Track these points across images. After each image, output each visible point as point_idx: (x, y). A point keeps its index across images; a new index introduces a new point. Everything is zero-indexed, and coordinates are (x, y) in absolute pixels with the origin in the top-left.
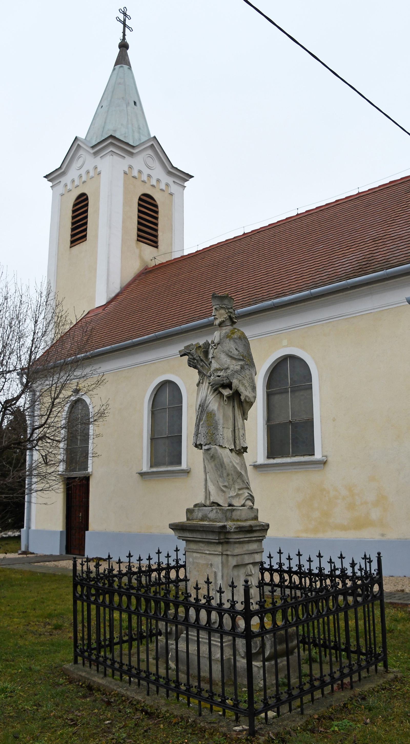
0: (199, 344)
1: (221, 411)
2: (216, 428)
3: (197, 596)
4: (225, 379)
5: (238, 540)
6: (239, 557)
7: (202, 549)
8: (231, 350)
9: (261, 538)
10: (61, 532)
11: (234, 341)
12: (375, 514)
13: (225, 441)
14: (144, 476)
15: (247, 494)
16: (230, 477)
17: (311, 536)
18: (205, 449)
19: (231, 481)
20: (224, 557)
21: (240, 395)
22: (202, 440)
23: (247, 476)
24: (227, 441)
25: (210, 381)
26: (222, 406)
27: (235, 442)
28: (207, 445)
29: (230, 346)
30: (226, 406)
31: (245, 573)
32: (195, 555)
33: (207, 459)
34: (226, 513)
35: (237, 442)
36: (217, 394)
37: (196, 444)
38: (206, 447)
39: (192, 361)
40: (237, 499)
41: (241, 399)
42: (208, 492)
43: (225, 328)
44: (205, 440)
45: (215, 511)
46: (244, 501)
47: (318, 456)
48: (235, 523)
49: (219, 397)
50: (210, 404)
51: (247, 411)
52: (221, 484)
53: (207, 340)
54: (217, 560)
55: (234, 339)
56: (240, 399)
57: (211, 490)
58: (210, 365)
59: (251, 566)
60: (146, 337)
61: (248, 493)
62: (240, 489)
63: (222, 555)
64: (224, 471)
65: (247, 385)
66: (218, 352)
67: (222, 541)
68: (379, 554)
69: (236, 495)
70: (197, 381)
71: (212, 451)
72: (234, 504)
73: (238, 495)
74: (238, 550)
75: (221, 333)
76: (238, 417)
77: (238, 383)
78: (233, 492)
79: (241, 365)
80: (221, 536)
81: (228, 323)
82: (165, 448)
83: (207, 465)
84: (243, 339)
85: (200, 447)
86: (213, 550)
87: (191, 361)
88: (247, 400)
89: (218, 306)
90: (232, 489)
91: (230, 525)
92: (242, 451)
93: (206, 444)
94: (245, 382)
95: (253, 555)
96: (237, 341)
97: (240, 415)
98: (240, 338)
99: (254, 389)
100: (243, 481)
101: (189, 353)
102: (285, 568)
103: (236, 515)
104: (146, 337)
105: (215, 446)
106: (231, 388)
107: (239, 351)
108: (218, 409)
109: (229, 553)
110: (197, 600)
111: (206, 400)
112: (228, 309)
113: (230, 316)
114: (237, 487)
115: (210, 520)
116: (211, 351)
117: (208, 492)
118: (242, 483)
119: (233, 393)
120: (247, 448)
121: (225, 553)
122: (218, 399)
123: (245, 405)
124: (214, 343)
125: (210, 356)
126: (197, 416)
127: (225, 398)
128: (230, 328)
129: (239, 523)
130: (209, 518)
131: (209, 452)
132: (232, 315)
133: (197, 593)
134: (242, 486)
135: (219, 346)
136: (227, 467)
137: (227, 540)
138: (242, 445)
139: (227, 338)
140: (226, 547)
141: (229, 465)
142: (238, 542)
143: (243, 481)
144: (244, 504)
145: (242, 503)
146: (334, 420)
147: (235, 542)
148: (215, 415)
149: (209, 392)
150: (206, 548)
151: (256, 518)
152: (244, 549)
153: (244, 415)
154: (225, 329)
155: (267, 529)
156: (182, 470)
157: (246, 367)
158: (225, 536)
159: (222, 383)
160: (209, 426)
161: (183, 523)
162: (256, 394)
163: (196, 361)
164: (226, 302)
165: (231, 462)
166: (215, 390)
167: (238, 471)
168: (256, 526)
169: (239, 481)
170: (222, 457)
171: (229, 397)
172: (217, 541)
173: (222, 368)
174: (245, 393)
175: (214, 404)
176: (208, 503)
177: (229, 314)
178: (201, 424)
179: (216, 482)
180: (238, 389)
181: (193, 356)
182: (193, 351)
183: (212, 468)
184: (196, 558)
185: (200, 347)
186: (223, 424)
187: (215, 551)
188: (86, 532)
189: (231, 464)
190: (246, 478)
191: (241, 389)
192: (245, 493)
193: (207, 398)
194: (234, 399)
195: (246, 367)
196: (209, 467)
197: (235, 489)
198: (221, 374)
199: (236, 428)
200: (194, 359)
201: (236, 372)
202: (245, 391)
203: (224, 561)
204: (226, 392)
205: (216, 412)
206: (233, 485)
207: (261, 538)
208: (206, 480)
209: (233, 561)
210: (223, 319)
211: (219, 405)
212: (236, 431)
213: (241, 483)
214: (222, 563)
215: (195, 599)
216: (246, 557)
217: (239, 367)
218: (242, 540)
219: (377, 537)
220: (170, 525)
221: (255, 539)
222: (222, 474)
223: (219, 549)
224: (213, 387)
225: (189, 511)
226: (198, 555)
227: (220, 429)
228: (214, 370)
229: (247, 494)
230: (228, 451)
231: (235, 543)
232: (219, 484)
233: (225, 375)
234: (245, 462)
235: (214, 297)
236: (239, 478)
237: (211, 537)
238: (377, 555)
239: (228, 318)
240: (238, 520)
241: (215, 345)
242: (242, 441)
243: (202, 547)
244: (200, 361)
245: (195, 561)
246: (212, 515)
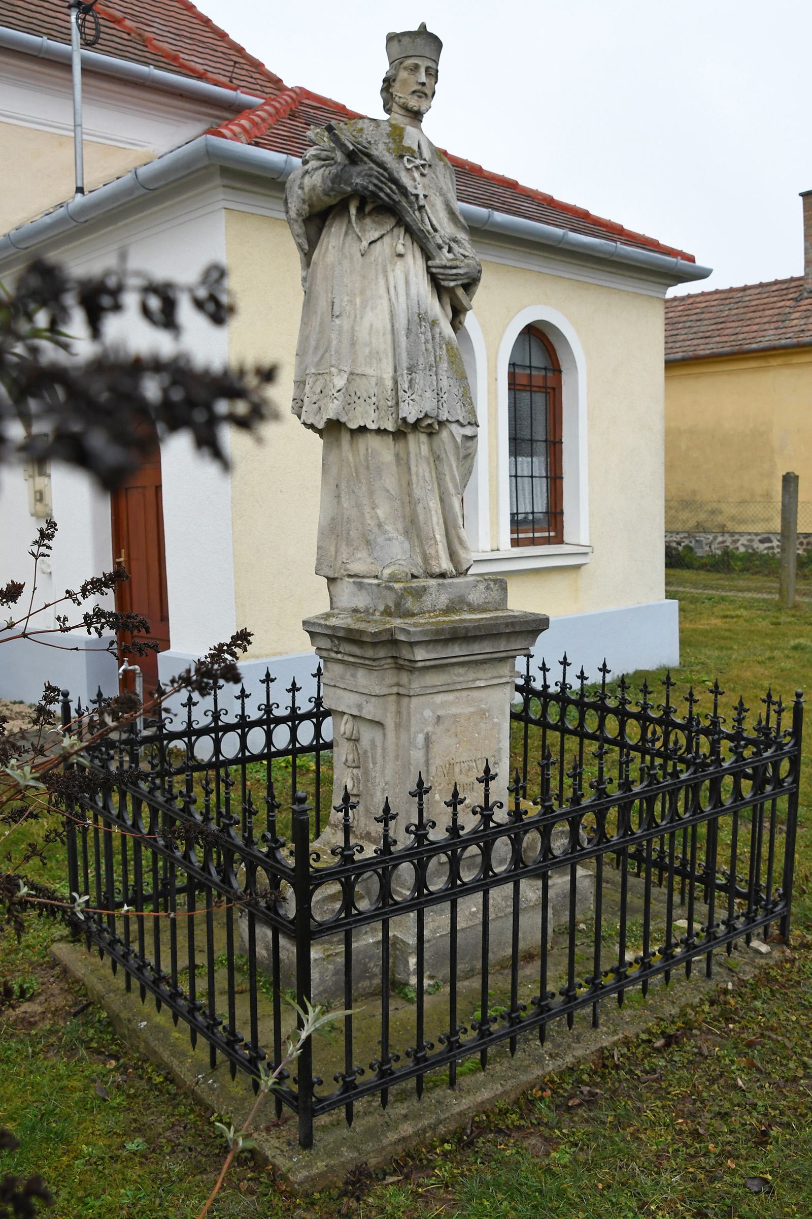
7: (461, 679)
28: (469, 427)
32: (439, 698)
115: (472, 609)
130: (469, 605)
150: (471, 675)
184: (443, 705)
187: (501, 677)
226: (450, 697)
243: (459, 675)
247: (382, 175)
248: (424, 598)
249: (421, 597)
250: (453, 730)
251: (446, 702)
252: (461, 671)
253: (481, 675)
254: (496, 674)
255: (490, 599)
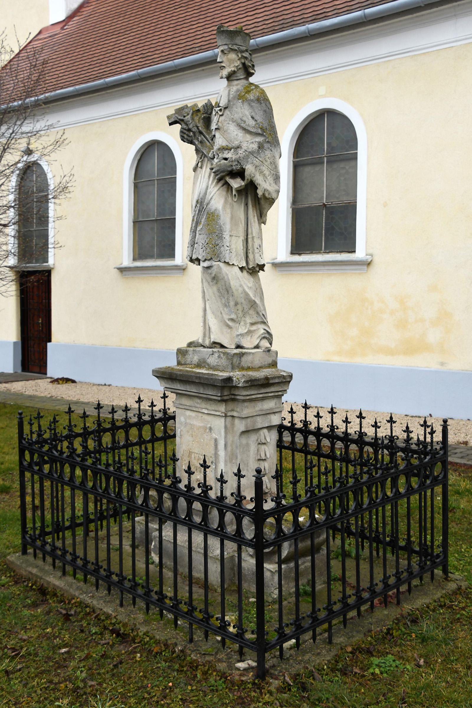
0: (197, 106)
1: (229, 211)
2: (220, 237)
3: (189, 482)
4: (234, 164)
5: (248, 398)
6: (249, 420)
7: (198, 406)
8: (244, 119)
9: (280, 393)
10: (15, 343)
11: (249, 104)
12: (434, 336)
13: (233, 256)
14: (124, 273)
15: (263, 331)
16: (239, 307)
17: (346, 360)
18: (204, 267)
19: (240, 311)
20: (229, 419)
21: (257, 188)
22: (200, 254)
23: (263, 305)
24: (236, 255)
25: (213, 167)
26: (230, 204)
27: (247, 257)
29: (243, 111)
30: (235, 204)
31: (257, 440)
32: (188, 413)
33: (207, 280)
34: (232, 359)
35: (251, 256)
36: (223, 186)
37: (191, 258)
38: (206, 264)
39: (187, 133)
40: (249, 338)
41: (257, 194)
42: (207, 327)
43: (236, 82)
44: (204, 254)
45: (216, 355)
46: (258, 341)
47: (360, 253)
48: (244, 373)
49: (226, 189)
50: (213, 200)
51: (266, 211)
52: (226, 317)
53: (209, 100)
54: (219, 424)
55: (249, 102)
56: (256, 194)
57: (211, 326)
58: (212, 140)
59: (265, 431)
60: (124, 76)
61: (265, 329)
62: (252, 324)
63: (226, 416)
64: (231, 298)
65: (267, 173)
66: (225, 121)
67: (225, 398)
68: (445, 421)
69: (246, 333)
70: (194, 163)
71: (214, 271)
72: (244, 345)
73: (249, 332)
74: (247, 410)
75: (229, 91)
76: (252, 221)
77: (254, 171)
78: (244, 328)
79: (259, 143)
80: (225, 392)
81: (241, 75)
82: (153, 235)
83: (207, 290)
84: (263, 101)
85: (196, 262)
86: (213, 409)
87: (185, 133)
88: (267, 195)
89: (226, 47)
90: (242, 323)
91: (238, 376)
92: (258, 269)
93: (205, 260)
94: (264, 168)
95: (268, 416)
96: (253, 104)
97: (256, 218)
98: (258, 100)
99: (277, 178)
100: (258, 313)
101: (182, 120)
102: (312, 427)
103: (246, 361)
104: (124, 76)
105: (219, 263)
106: (243, 178)
107: (256, 121)
108: (224, 207)
109: (235, 414)
110: (189, 487)
111: (206, 193)
112: (242, 52)
113: (244, 64)
114: (249, 320)
116: (215, 119)
117: (207, 327)
118: (256, 315)
119: (246, 185)
120: (264, 265)
121: (229, 414)
122: (224, 193)
123: (262, 202)
124: (219, 107)
125: (213, 126)
126: (194, 217)
127: (234, 192)
128: (244, 82)
129: (251, 373)
130: (208, 365)
131: (210, 271)
132: (247, 62)
133: (189, 479)
134: (255, 319)
135: (227, 112)
136: (235, 293)
137: (233, 397)
138: (257, 262)
139: (239, 99)
140: (231, 405)
141: (237, 290)
142: (249, 399)
143: (258, 313)
144: (258, 345)
145: (256, 343)
146: (385, 205)
147: (243, 400)
148: (218, 216)
149: (210, 182)
150: (203, 405)
151: (274, 364)
152: (257, 409)
153: (261, 217)
154: (237, 85)
155: (290, 381)
156: (176, 266)
157: (266, 145)
158: (230, 391)
159: (229, 169)
160: (211, 233)
161: (173, 369)
162: (279, 187)
163: (191, 134)
164: (238, 40)
165: (241, 286)
166: (220, 180)
167: (251, 299)
168: (274, 378)
169: (252, 312)
170: (228, 279)
171: (240, 191)
172: (219, 398)
173: (230, 146)
174: (264, 185)
175: (218, 200)
176: (207, 343)
177: (243, 61)
178: (198, 229)
179: (219, 314)
180: (254, 179)
181: (187, 125)
182: (188, 118)
183: (214, 294)
185: (198, 111)
186: (230, 231)
187: (216, 411)
188: (49, 344)
189: (240, 289)
190: (262, 308)
191: (259, 180)
192: (259, 329)
193: (208, 191)
194: (247, 193)
195: (266, 145)
196: (211, 291)
197: (245, 324)
198: (229, 155)
199: (249, 236)
200: (189, 130)
201: (252, 153)
202: (264, 183)
203: (229, 425)
204: (236, 184)
205: (221, 213)
206: (243, 319)
207: (280, 393)
208: (205, 310)
209: (240, 426)
210: (233, 69)
211: (226, 202)
212: (250, 240)
213: (255, 316)
214: (226, 427)
215: (186, 486)
216: (259, 419)
217: (255, 146)
218: (253, 397)
219: (434, 366)
220: (153, 371)
221: (272, 394)
222: (228, 303)
223: (222, 408)
224: (217, 175)
225: (181, 352)
226: (193, 414)
227: (227, 238)
228: (219, 149)
229: (263, 331)
230: (237, 269)
231: (244, 401)
232: (223, 317)
233: (234, 157)
234: (260, 285)
235: (221, 31)
236: (253, 308)
237: (210, 392)
238: (442, 423)
239: (241, 66)
240: (249, 369)
241: (220, 110)
242: (257, 256)
243: (198, 403)
244: (197, 134)
245: (187, 421)
246: (213, 360)
247: (185, 129)
248: (186, 356)
249: (185, 355)
250: (190, 432)
251: (191, 416)
252: (199, 401)
253: (208, 406)
254: (217, 409)
255: (220, 364)
